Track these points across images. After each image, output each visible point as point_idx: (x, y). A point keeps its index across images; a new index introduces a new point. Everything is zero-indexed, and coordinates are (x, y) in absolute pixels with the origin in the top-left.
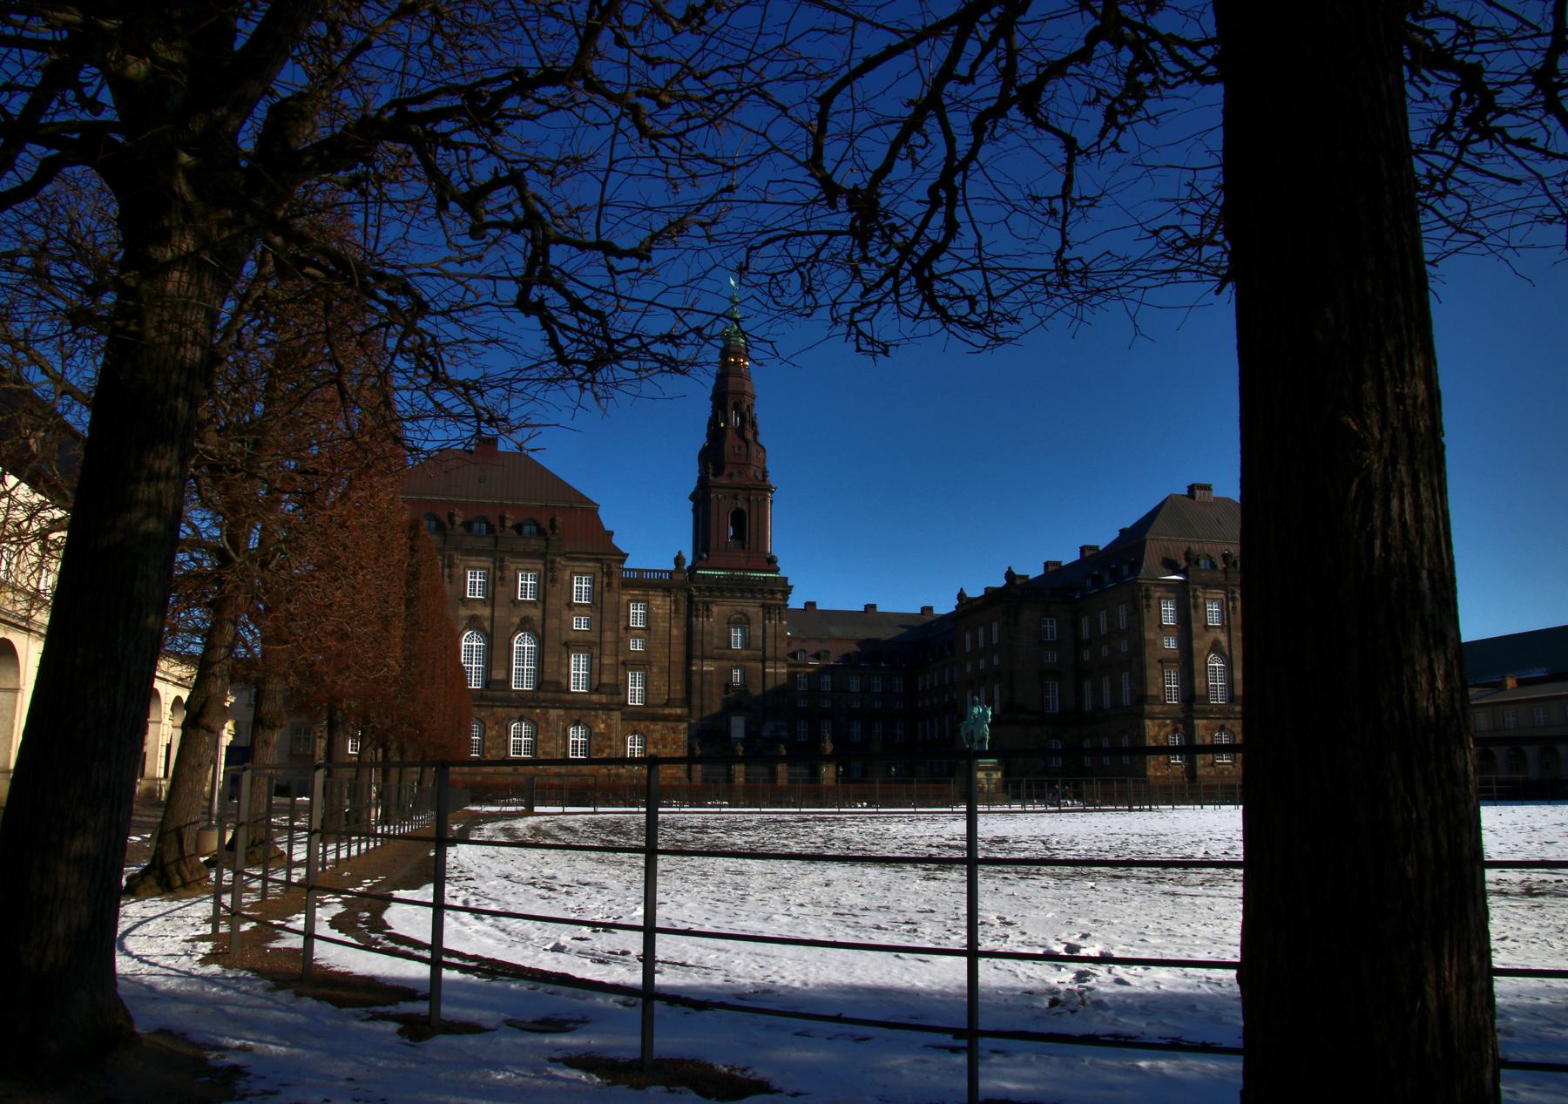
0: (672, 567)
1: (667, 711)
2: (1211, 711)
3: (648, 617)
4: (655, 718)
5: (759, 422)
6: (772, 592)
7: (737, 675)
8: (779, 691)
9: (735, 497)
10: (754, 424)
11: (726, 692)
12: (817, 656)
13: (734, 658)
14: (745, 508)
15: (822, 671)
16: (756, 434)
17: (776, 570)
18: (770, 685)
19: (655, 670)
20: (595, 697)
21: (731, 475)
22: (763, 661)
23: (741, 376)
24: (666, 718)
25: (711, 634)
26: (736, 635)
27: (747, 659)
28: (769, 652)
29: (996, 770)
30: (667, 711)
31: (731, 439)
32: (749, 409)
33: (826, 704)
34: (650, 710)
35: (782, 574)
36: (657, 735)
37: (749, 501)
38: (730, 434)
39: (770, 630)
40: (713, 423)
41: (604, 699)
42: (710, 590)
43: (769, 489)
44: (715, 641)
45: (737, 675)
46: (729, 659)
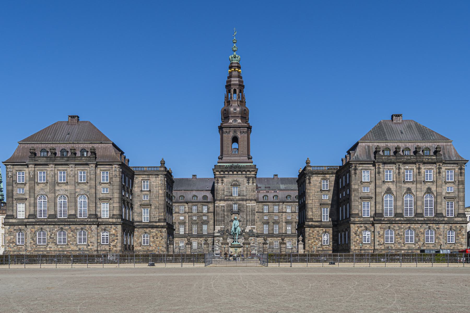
0: (160, 165)
1: (158, 224)
2: (384, 220)
4: (153, 227)
19: (153, 207)
20: (111, 220)
24: (157, 227)
25: (224, 190)
27: (239, 200)
34: (151, 224)
36: (154, 234)
41: (114, 220)
44: (225, 193)
45: (235, 207)
46: (231, 200)
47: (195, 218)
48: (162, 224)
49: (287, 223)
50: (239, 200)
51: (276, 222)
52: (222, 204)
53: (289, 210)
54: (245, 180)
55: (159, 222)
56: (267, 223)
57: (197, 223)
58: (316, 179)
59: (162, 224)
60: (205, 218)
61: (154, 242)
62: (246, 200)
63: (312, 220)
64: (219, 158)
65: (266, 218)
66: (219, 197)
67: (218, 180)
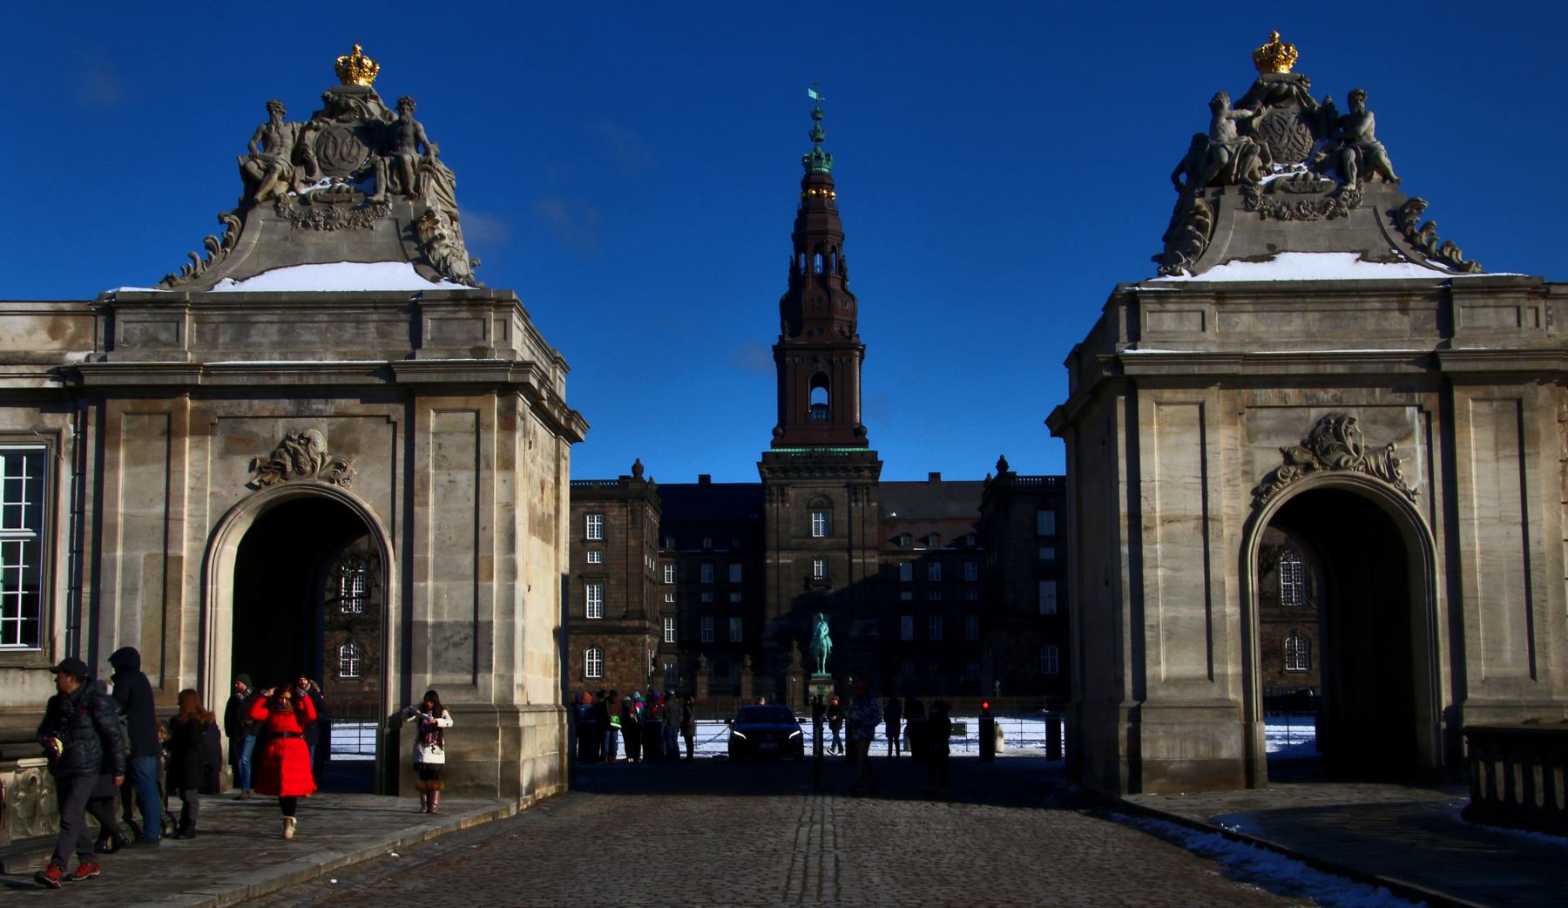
1: (625, 624)
3: (604, 530)
4: (613, 631)
5: (848, 265)
6: (858, 470)
7: (818, 568)
8: (869, 583)
9: (815, 360)
10: (841, 269)
11: (807, 587)
12: (925, 541)
13: (815, 548)
14: (828, 372)
15: (929, 557)
16: (844, 279)
17: (865, 444)
18: (858, 576)
19: (613, 582)
21: (810, 334)
22: (850, 550)
23: (823, 210)
26: (817, 522)
27: (832, 548)
28: (856, 539)
29: (829, 683)
30: (625, 624)
31: (811, 290)
32: (834, 249)
33: (935, 597)
34: (608, 624)
35: (871, 448)
37: (831, 363)
38: (810, 282)
39: (857, 514)
40: (794, 269)
42: (785, 471)
43: (855, 347)
44: (793, 529)
45: (818, 568)
46: (810, 549)
48: (637, 623)
50: (832, 548)
55: (625, 618)
59: (637, 623)
60: (734, 598)
61: (614, 669)
64: (775, 432)
65: (907, 596)
66: (771, 539)
67: (770, 494)
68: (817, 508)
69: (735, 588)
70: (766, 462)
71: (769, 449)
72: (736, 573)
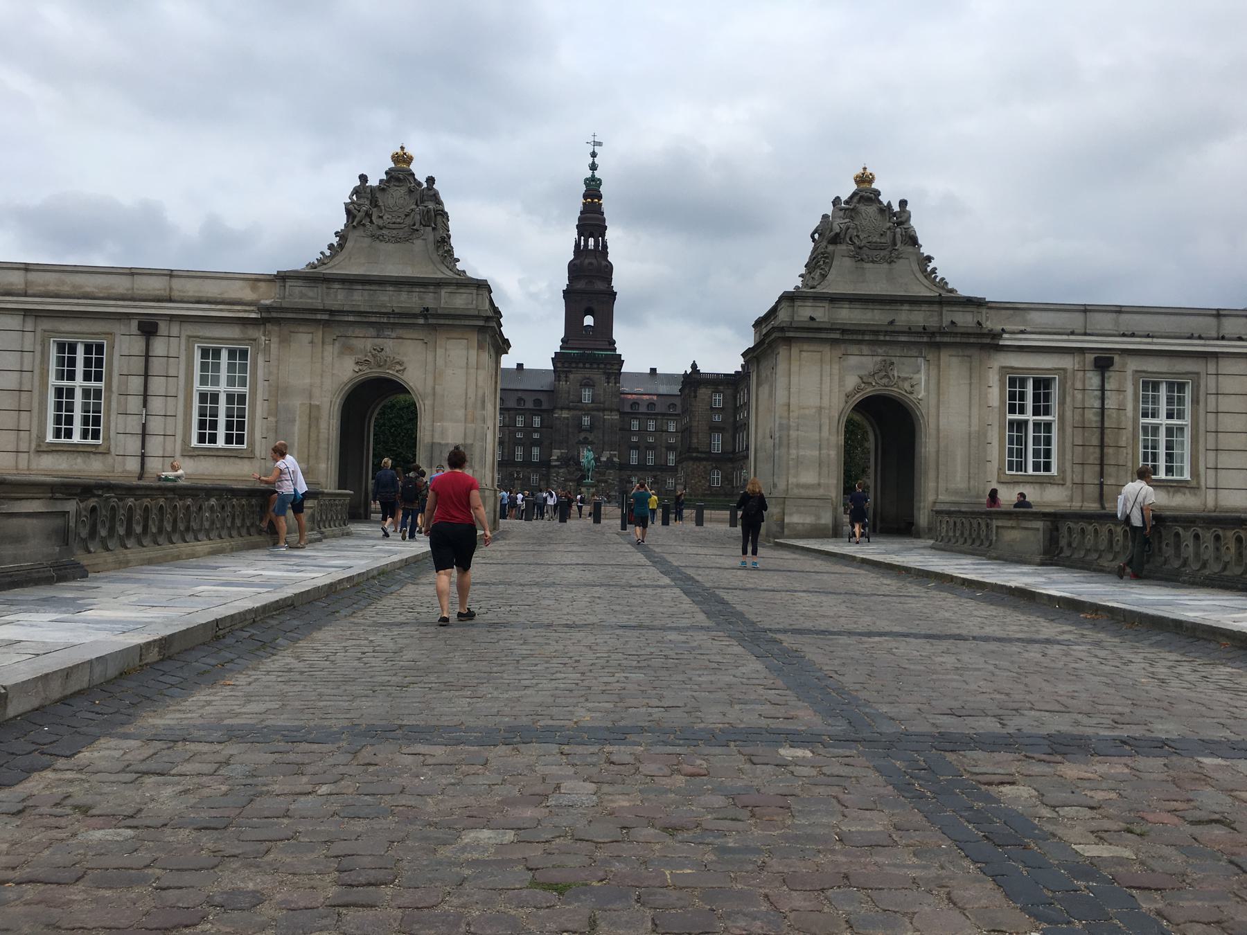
10: (605, 247)
17: (615, 349)
27: (593, 410)
40: (577, 245)
45: (586, 420)
47: (519, 436)
49: (670, 448)
50: (593, 410)
51: (650, 447)
52: (565, 414)
53: (672, 429)
54: (603, 378)
56: (636, 447)
57: (522, 445)
58: (703, 392)
60: (536, 436)
62: (604, 410)
63: (697, 450)
65: (635, 439)
68: (587, 385)
69: (536, 430)
70: (557, 359)
71: (558, 350)
72: (537, 421)
